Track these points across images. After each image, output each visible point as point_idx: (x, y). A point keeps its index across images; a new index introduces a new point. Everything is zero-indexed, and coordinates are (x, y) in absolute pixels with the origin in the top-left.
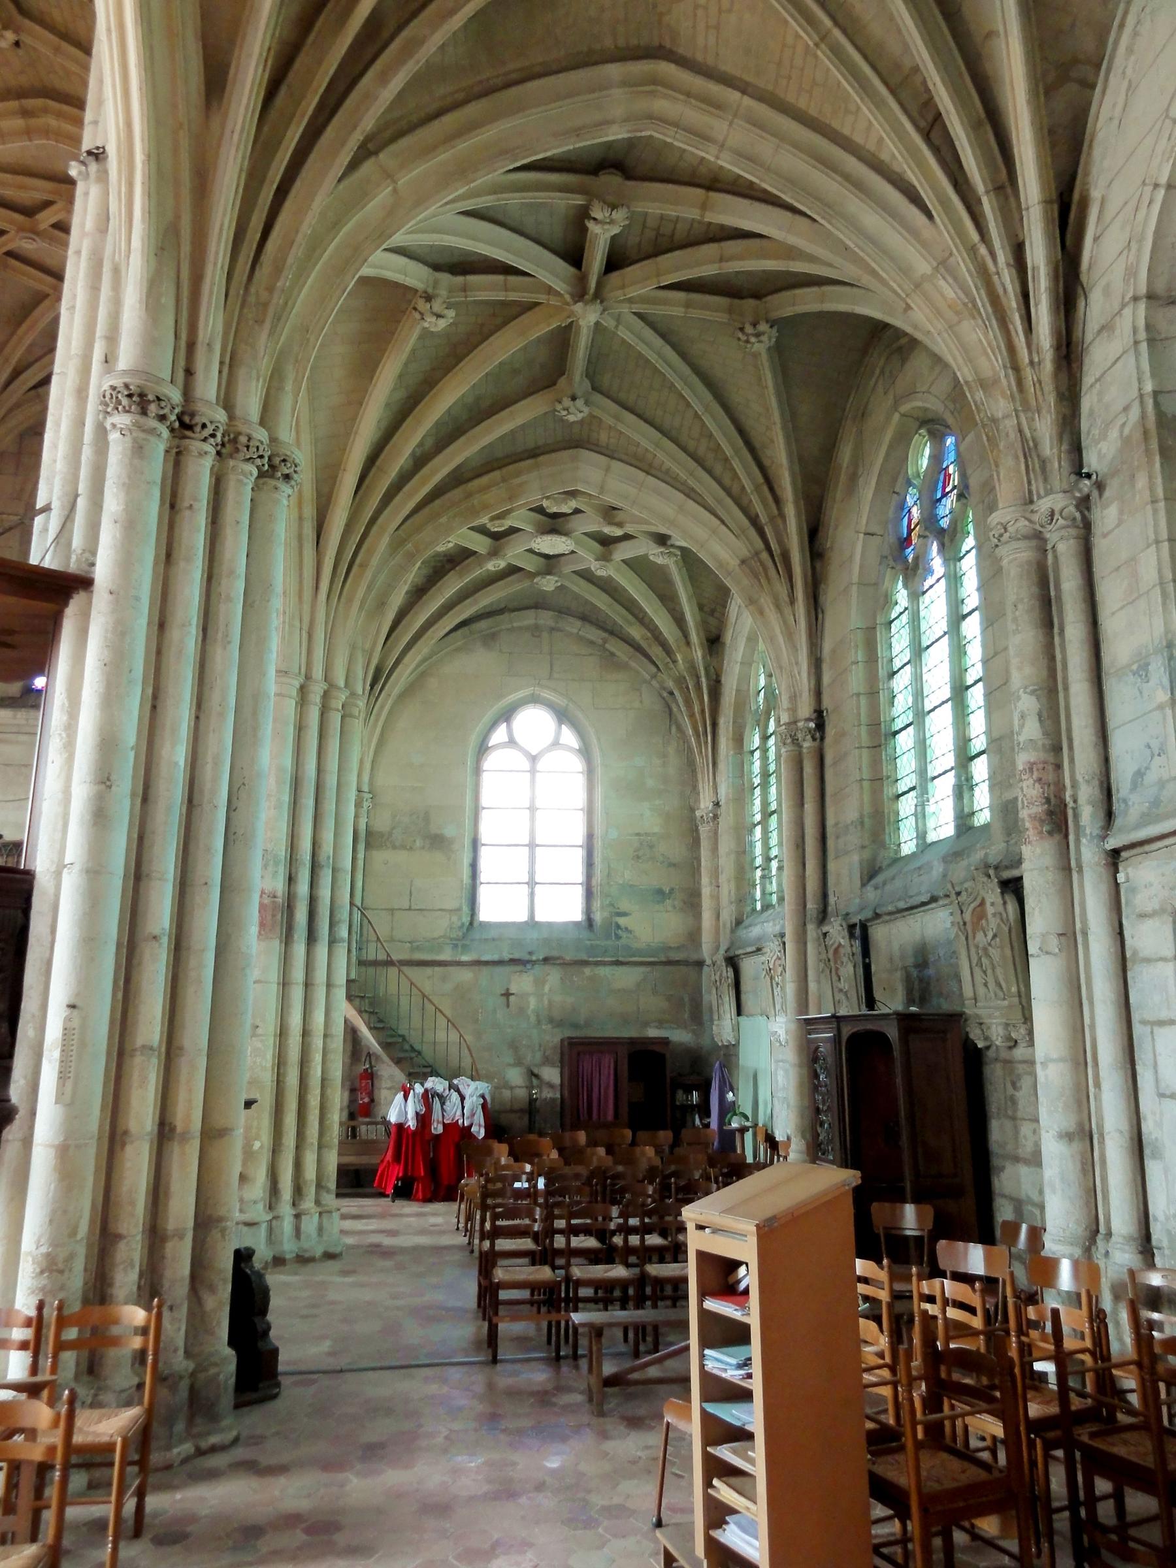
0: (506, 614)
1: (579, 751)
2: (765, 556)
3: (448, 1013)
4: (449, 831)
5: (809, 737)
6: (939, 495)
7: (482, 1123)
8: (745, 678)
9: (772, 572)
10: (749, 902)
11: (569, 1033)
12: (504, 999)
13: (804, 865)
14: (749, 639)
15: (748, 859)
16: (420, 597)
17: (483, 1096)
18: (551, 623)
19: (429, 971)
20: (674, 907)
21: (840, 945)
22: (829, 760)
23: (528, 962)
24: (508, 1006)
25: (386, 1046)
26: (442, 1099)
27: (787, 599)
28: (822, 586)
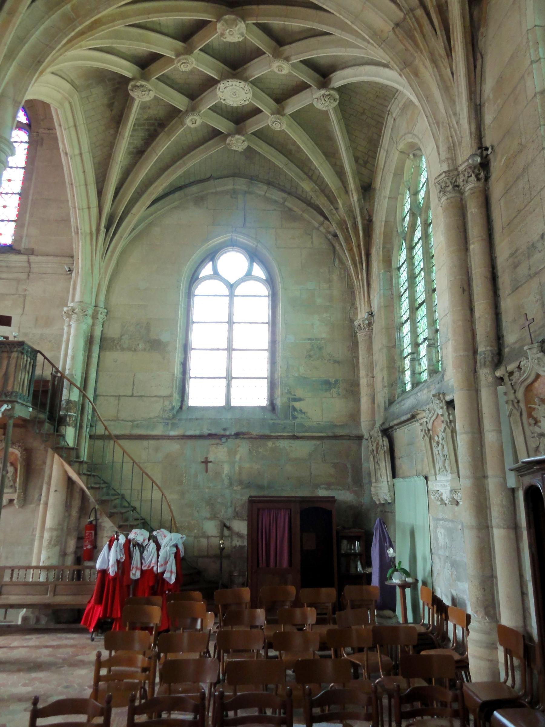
0: (211, 182)
1: (266, 280)
2: (420, 12)
3: (158, 478)
4: (165, 337)
5: (473, 177)
7: (174, 569)
8: (393, 210)
9: (427, 28)
10: (399, 385)
11: (254, 493)
12: (204, 465)
13: (472, 310)
14: (395, 174)
15: (398, 351)
16: (140, 158)
17: (176, 546)
18: (244, 188)
19: (145, 443)
20: (339, 394)
21: (538, 376)
22: (497, 190)
23: (224, 436)
24: (207, 471)
25: (102, 502)
26: (142, 548)
27: (443, 52)
28: (482, 30)
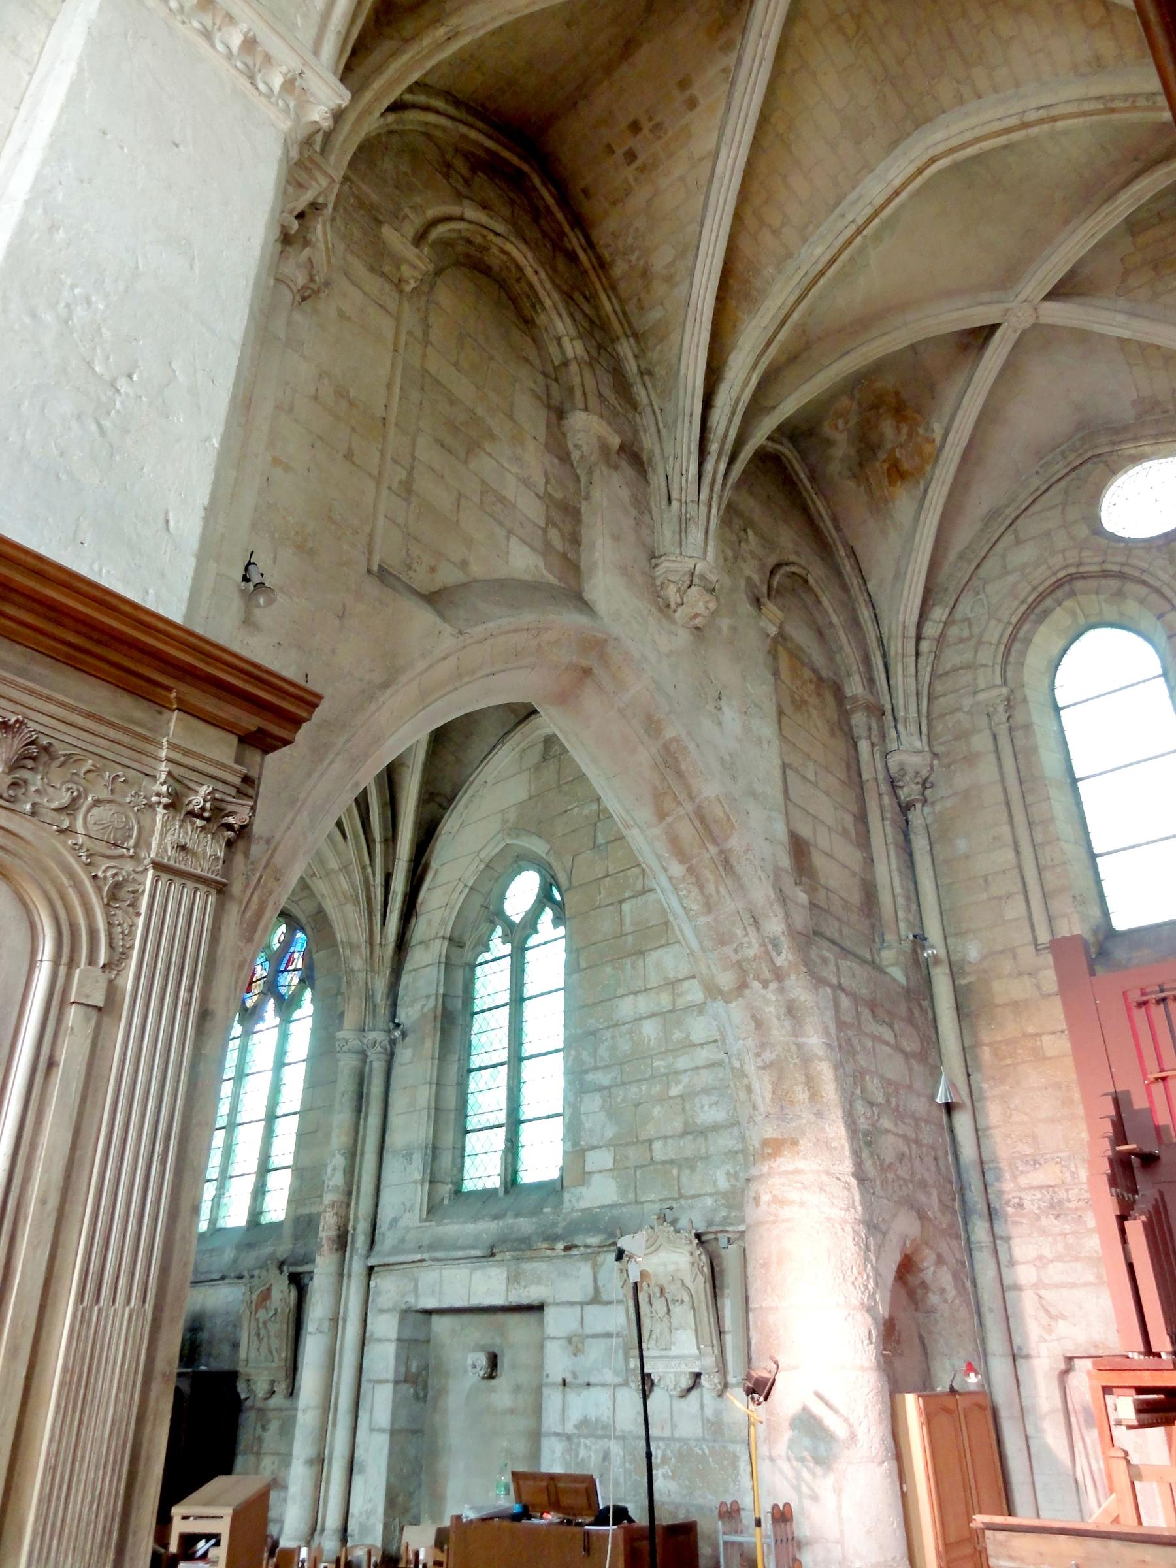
6: (282, 968)
